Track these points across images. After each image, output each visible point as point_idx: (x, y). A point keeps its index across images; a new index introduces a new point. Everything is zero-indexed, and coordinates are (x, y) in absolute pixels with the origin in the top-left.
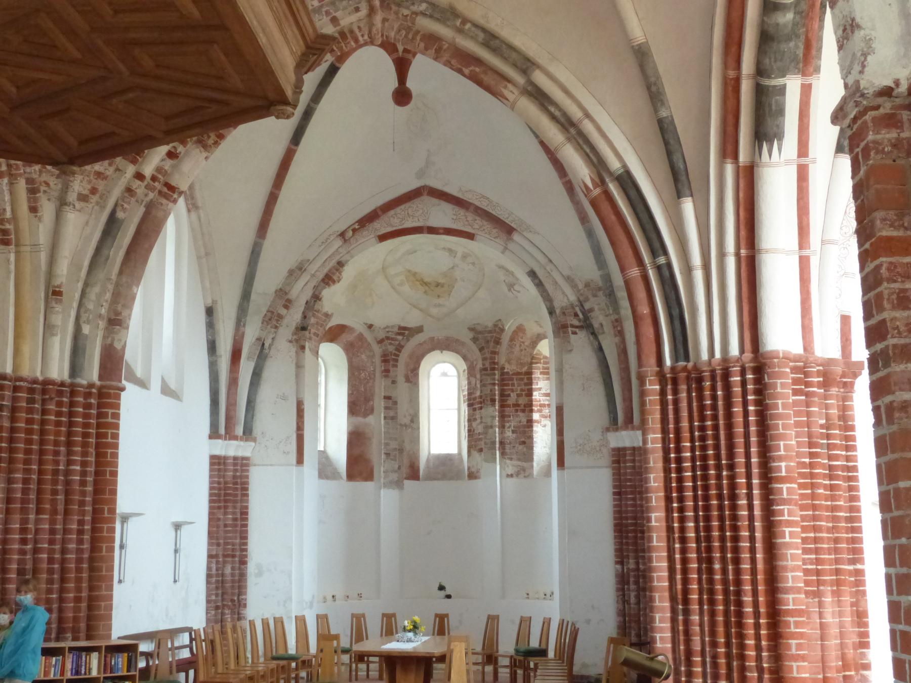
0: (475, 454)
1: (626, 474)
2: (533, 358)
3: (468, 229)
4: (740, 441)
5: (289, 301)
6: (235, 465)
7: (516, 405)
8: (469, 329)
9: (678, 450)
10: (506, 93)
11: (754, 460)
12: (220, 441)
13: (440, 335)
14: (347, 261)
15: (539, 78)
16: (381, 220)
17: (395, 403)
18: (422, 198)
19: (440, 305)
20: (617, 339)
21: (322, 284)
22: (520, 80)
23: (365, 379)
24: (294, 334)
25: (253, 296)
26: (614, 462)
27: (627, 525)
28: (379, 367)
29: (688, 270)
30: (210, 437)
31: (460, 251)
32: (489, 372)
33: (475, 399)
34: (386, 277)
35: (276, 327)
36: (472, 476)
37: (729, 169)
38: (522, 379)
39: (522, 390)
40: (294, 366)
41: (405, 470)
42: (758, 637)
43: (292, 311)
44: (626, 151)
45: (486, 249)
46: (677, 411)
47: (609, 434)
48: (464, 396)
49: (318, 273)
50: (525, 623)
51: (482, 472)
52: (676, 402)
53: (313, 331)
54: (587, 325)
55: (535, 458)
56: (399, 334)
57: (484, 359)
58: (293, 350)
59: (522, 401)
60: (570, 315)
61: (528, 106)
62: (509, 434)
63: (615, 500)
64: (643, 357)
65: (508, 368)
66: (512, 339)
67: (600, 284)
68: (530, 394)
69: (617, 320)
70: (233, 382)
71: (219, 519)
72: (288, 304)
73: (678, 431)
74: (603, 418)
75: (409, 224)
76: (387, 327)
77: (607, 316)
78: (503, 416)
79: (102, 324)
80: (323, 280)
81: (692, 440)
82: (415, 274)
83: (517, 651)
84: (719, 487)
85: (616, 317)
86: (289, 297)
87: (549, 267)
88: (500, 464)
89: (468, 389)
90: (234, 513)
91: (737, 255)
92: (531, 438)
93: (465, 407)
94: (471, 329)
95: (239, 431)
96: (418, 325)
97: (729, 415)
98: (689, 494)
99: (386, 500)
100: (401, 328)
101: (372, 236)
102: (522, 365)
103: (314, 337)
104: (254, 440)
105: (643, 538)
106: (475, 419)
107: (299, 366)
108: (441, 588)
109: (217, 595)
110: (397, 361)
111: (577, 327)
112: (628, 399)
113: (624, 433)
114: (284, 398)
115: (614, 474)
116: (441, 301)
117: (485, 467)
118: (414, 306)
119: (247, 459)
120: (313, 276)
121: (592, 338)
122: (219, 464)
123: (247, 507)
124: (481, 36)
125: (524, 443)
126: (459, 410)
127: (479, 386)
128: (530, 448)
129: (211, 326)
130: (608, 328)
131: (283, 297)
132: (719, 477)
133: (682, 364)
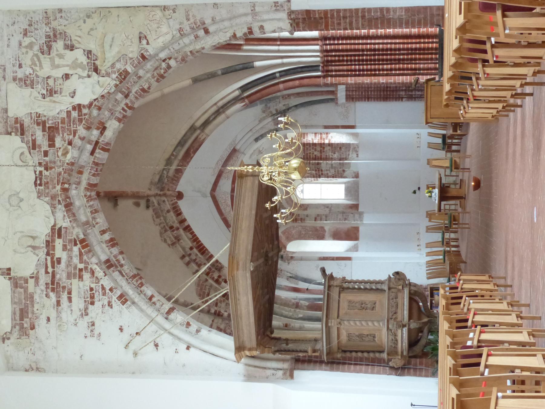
0: (345, 174)
1: (359, 95)
4: (353, 47)
7: (321, 152)
9: (355, 70)
10: (202, 138)
11: (361, 41)
15: (198, 124)
17: (318, 215)
20: (292, 97)
22: (198, 132)
24: (285, 261)
26: (353, 101)
27: (384, 95)
28: (299, 223)
29: (283, 65)
33: (316, 174)
36: (357, 176)
37: (245, 47)
38: (307, 149)
39: (313, 149)
40: (302, 262)
41: (354, 211)
42: (428, 43)
44: (232, 89)
46: (339, 71)
48: (314, 180)
50: (431, 146)
51: (355, 170)
52: (336, 71)
55: (348, 142)
58: (293, 262)
59: (318, 148)
61: (207, 130)
62: (335, 156)
63: (371, 101)
64: (316, 83)
67: (263, 105)
69: (283, 97)
73: (348, 71)
74: (330, 105)
78: (326, 159)
79: (298, 310)
81: (352, 65)
83: (443, 149)
84: (370, 55)
87: (254, 131)
89: (311, 177)
91: (279, 45)
92: (338, 144)
93: (321, 180)
97: (342, 51)
98: (373, 67)
99: (368, 221)
105: (390, 87)
106: (327, 174)
107: (301, 259)
108: (415, 192)
112: (322, 93)
113: (339, 95)
115: (359, 101)
117: (353, 169)
124: (179, 148)
125: (340, 148)
128: (343, 144)
130: (286, 102)
132: (367, 55)
133: (320, 68)
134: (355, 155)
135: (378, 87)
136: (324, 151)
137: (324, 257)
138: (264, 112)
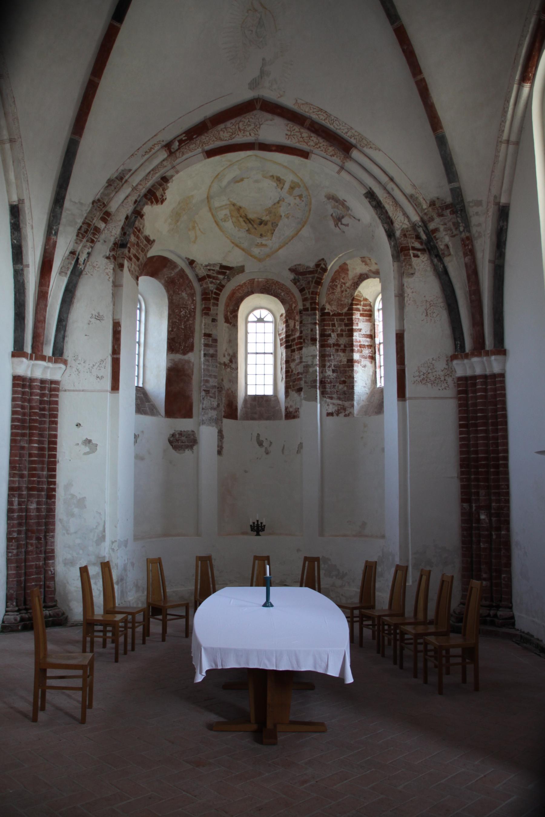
0: (294, 394)
1: (475, 405)
2: (353, 299)
3: (304, 147)
5: (108, 214)
8: (290, 269)
12: (24, 360)
13: (260, 278)
14: (172, 176)
17: (215, 341)
18: (255, 112)
19: (262, 245)
21: (144, 199)
23: (185, 316)
24: (112, 249)
25: (67, 204)
26: (459, 392)
30: (14, 355)
31: (289, 178)
33: (294, 340)
34: (210, 209)
35: (92, 241)
36: (291, 415)
38: (342, 320)
39: (342, 330)
40: (110, 284)
41: (222, 408)
43: (111, 225)
45: (321, 170)
47: (455, 362)
48: (281, 340)
49: (140, 187)
51: (302, 412)
53: (133, 251)
54: (431, 248)
55: (356, 397)
56: (219, 273)
57: (305, 300)
59: (343, 341)
60: (413, 238)
62: (329, 373)
63: (461, 433)
65: (328, 308)
66: (333, 280)
68: (350, 333)
69: (468, 238)
70: (42, 296)
71: (23, 448)
72: (106, 217)
74: (446, 345)
75: (240, 139)
76: (209, 265)
77: (454, 236)
78: (323, 356)
80: (145, 196)
82: (239, 209)
85: (467, 234)
87: (390, 186)
88: (320, 403)
89: (286, 332)
90: (40, 442)
92: (352, 377)
93: (282, 351)
94: (291, 270)
95: (48, 351)
100: (222, 267)
101: (200, 150)
102: (342, 306)
103: (134, 259)
104: (65, 362)
106: (294, 360)
107: (116, 285)
109: (19, 532)
110: (217, 299)
111: (418, 250)
113: (475, 359)
114: (99, 318)
115: (460, 406)
116: (264, 241)
117: (305, 407)
118: (237, 246)
119: (57, 383)
120: (134, 189)
121: (435, 260)
122: (24, 386)
123: (56, 436)
125: (344, 382)
126: (275, 354)
127: (298, 327)
128: (351, 387)
131: (101, 208)
134: (331, 409)
135: (497, 445)
136: (337, 350)
138: (432, 204)
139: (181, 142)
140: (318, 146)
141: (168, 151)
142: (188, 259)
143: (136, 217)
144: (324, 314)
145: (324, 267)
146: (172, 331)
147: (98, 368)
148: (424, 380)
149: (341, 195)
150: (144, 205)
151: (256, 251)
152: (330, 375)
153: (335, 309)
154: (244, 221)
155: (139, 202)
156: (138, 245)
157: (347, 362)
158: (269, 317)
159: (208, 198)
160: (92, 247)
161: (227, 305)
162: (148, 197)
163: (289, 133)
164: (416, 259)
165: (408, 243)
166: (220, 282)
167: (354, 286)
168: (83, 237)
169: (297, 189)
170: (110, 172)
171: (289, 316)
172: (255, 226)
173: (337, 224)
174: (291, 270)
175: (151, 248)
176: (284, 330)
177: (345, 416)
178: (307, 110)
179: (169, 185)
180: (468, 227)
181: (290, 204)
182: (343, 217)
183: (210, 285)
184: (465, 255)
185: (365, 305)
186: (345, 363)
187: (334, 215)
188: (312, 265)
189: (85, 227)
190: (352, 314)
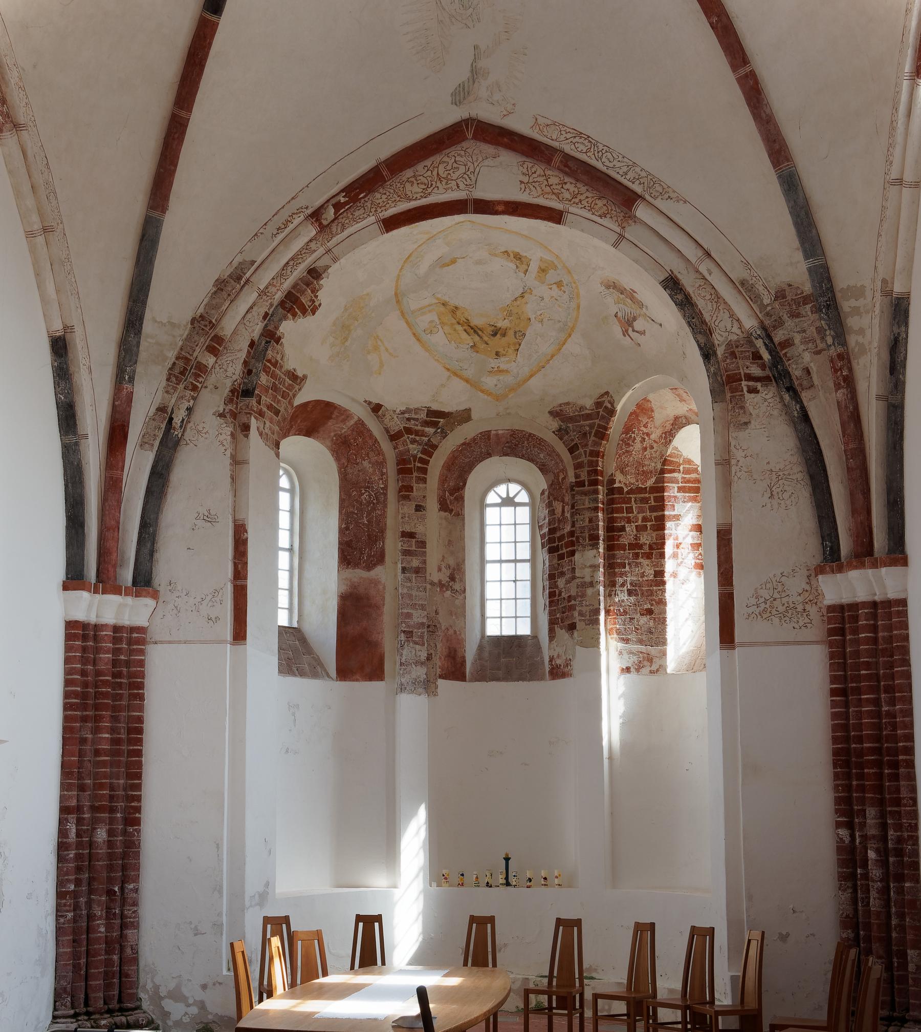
0: (562, 633)
2: (665, 462)
5: (218, 339)
6: (116, 640)
7: (635, 546)
8: (550, 413)
12: (85, 594)
13: (501, 426)
14: (327, 267)
16: (390, 185)
17: (422, 544)
19: (500, 371)
23: (369, 503)
24: (229, 401)
25: (148, 327)
27: (860, 753)
30: (66, 587)
32: (586, 488)
34: (403, 314)
35: (195, 388)
39: (645, 519)
40: (228, 461)
41: (438, 662)
43: (225, 359)
48: (543, 537)
49: (272, 289)
51: (576, 665)
54: (779, 375)
56: (426, 424)
57: (578, 466)
59: (646, 539)
60: (747, 358)
65: (621, 480)
66: (628, 429)
68: (660, 525)
69: (840, 357)
70: (112, 486)
71: (83, 741)
72: (216, 346)
74: (809, 548)
77: (818, 353)
78: (611, 566)
80: (282, 304)
82: (455, 310)
85: (840, 349)
86: (217, 331)
89: (550, 523)
90: (113, 730)
92: (662, 602)
93: (543, 556)
94: (554, 414)
95: (127, 575)
96: (462, 408)
100: (432, 413)
101: (372, 219)
102: (646, 474)
103: (269, 414)
104: (155, 595)
105: (895, 777)
106: (562, 574)
107: (238, 462)
109: (78, 883)
110: (425, 471)
111: (757, 379)
114: (209, 518)
116: (502, 363)
118: (456, 374)
119: (141, 630)
120: (263, 293)
121: (787, 397)
122: (85, 638)
123: (140, 720)
125: (650, 612)
126: (533, 561)
127: (568, 515)
129: (63, 374)
135: (894, 727)
137: (245, 542)
139: (338, 206)
140: (577, 200)
141: (317, 225)
142: (370, 403)
143: (267, 342)
144: (611, 491)
145: (609, 406)
146: (347, 528)
147: (211, 604)
148: (766, 612)
149: (628, 282)
150: (280, 320)
151: (489, 382)
152: (623, 601)
153: (633, 481)
154: (465, 330)
155: (272, 316)
156: (275, 388)
157: (655, 577)
158: (523, 497)
159: (396, 294)
160: (194, 399)
161: (443, 480)
162: (287, 305)
163: (526, 179)
164: (753, 395)
165: (738, 368)
166: (429, 440)
167: (666, 438)
168: (179, 382)
169: (551, 271)
170: (220, 268)
171: (553, 494)
172: (486, 338)
173: (627, 331)
174: (554, 414)
175: (300, 390)
176: (547, 520)
177: (651, 672)
178: (554, 137)
179: (321, 282)
180: (841, 336)
181: (543, 299)
182: (635, 319)
183: (411, 446)
184: (838, 387)
185: (687, 472)
186: (651, 577)
187: (619, 314)
188: (589, 403)
189: (181, 363)
190: (662, 489)
